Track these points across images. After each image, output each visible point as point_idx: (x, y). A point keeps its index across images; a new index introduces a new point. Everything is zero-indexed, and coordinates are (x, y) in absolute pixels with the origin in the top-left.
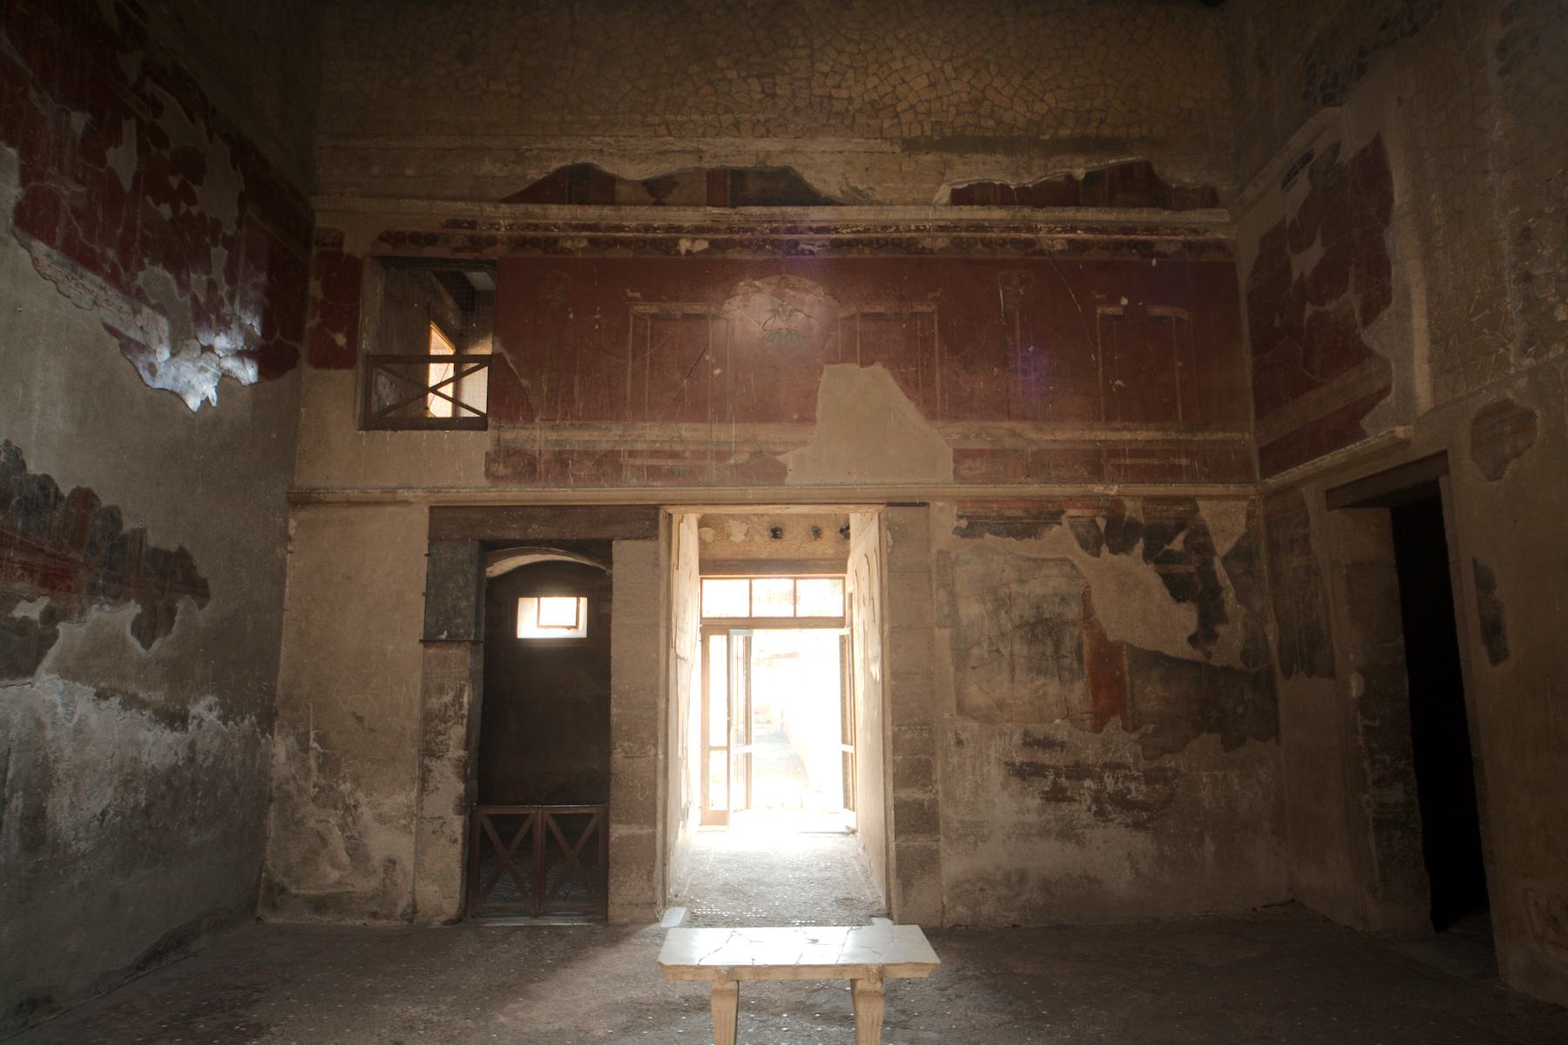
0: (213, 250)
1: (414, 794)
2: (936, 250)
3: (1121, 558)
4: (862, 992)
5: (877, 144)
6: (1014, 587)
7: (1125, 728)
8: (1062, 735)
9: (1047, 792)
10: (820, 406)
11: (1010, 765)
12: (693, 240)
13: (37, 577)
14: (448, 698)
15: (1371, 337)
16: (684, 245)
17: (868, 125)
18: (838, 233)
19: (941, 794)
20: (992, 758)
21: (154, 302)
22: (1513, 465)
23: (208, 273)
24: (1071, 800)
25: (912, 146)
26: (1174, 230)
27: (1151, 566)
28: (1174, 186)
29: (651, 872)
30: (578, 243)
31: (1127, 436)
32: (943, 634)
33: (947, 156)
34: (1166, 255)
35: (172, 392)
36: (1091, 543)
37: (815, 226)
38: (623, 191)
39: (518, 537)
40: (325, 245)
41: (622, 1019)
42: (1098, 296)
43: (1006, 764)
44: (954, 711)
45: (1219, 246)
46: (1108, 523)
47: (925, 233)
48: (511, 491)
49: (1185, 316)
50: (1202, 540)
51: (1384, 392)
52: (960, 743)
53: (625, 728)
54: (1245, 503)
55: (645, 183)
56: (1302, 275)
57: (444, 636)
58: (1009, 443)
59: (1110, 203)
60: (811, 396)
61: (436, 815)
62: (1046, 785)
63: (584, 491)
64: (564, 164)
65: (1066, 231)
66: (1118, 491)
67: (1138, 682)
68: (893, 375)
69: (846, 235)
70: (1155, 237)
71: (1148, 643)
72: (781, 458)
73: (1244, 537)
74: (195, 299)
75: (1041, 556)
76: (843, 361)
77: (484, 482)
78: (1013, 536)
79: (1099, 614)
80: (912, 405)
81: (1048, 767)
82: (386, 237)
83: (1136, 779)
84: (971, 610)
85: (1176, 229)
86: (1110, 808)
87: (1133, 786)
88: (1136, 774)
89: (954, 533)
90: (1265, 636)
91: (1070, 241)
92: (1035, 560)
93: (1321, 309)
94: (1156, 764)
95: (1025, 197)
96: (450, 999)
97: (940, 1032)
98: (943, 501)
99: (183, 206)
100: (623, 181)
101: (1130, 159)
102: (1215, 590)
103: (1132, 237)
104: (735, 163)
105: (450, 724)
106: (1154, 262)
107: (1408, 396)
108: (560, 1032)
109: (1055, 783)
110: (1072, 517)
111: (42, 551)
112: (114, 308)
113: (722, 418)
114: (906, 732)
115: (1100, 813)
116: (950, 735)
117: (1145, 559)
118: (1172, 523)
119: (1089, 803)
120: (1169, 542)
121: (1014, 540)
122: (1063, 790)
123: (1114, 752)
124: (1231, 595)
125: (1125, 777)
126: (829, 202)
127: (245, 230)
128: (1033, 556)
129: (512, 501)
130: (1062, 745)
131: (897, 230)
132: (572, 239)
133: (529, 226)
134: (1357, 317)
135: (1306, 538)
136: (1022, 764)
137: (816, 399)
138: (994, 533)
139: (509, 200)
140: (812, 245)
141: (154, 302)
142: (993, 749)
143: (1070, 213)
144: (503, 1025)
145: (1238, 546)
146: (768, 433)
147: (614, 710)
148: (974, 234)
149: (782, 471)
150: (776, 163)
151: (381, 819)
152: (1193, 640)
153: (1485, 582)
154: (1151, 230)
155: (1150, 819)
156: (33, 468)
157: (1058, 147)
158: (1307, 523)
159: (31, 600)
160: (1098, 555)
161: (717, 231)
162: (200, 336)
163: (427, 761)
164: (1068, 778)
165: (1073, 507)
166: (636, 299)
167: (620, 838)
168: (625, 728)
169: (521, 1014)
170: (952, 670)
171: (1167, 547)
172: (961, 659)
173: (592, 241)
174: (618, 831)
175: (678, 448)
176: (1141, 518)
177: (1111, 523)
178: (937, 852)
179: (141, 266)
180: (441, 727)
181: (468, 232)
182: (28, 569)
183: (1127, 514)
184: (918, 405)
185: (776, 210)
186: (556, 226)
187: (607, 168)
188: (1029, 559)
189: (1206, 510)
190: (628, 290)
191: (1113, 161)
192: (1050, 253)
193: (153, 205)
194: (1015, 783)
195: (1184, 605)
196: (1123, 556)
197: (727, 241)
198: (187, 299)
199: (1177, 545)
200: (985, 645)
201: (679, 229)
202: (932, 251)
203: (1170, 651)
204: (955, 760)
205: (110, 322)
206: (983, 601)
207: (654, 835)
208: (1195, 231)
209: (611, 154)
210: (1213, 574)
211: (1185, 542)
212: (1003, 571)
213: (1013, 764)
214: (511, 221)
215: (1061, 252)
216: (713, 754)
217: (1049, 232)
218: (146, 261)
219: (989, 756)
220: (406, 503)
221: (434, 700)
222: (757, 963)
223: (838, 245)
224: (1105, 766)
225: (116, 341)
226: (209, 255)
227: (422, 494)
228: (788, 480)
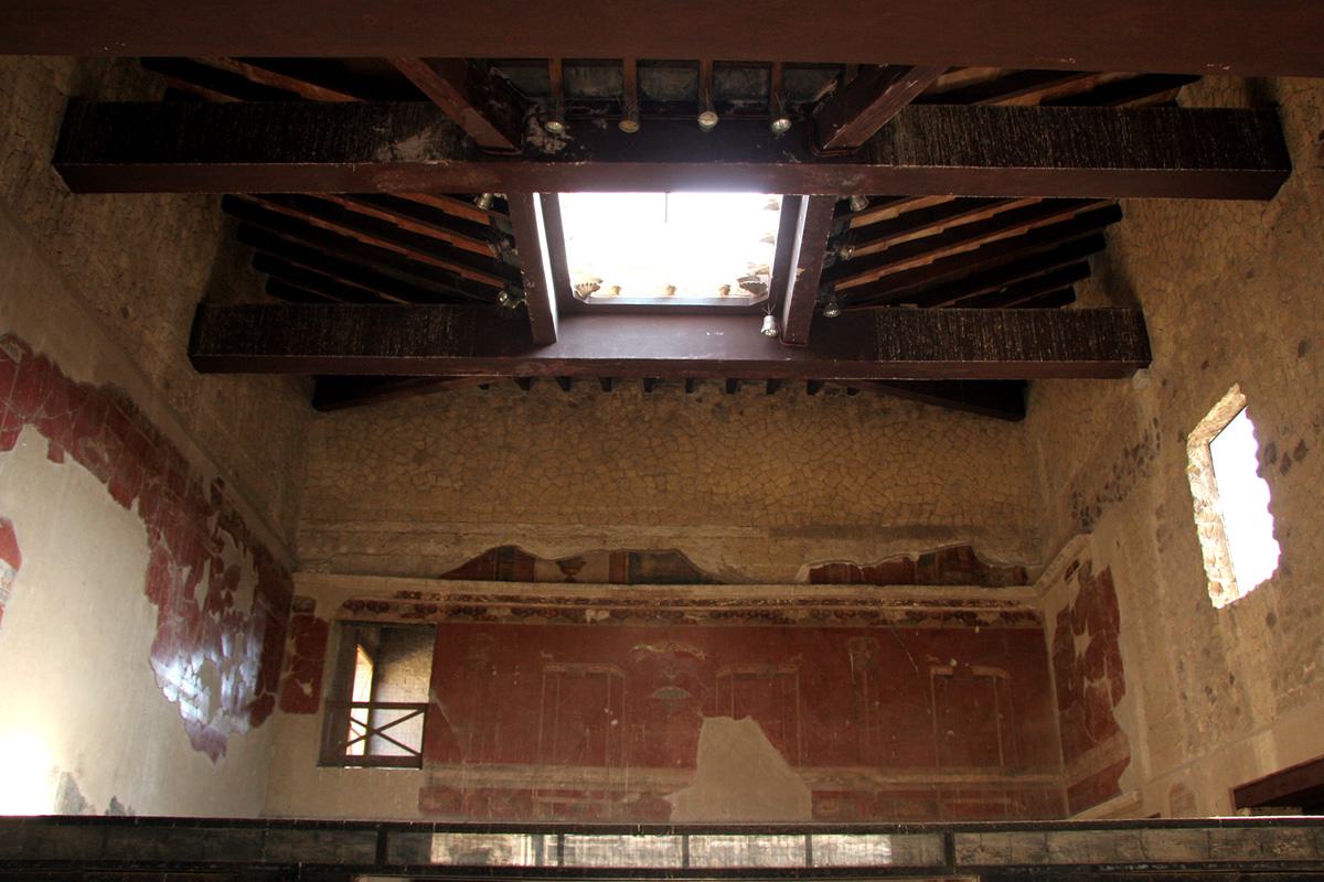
2: (797, 620)
12: (597, 611)
16: (590, 614)
17: (742, 516)
18: (716, 605)
26: (993, 603)
28: (991, 566)
30: (502, 612)
34: (986, 624)
37: (697, 599)
38: (540, 569)
40: (300, 610)
45: (1030, 616)
47: (788, 607)
55: (559, 562)
64: (493, 546)
69: (722, 608)
70: (977, 609)
82: (348, 605)
85: (994, 601)
91: (908, 613)
100: (541, 560)
101: (956, 543)
103: (959, 609)
106: (977, 629)
126: (708, 580)
132: (498, 608)
140: (695, 615)
148: (830, 607)
154: (973, 603)
157: (898, 533)
166: (548, 660)
173: (514, 610)
181: (414, 602)
185: (665, 587)
186: (485, 597)
190: (542, 652)
191: (942, 545)
192: (892, 623)
201: (586, 601)
202: (794, 622)
208: (1010, 603)
209: (532, 539)
214: (449, 593)
215: (900, 621)
217: (890, 605)
223: (717, 615)
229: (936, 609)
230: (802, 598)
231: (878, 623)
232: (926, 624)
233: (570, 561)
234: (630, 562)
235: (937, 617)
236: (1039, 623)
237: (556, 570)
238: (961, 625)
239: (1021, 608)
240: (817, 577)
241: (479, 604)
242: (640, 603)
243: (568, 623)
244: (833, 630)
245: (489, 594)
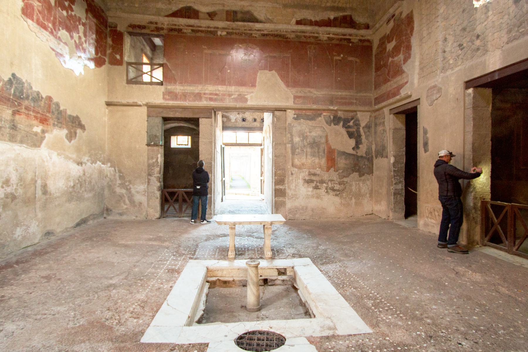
0: (79, 27)
3: (337, 127)
4: (267, 228)
5: (275, 5)
6: (308, 134)
7: (334, 171)
8: (318, 172)
10: (257, 82)
11: (305, 180)
12: (222, 32)
13: (39, 120)
15: (405, 68)
21: (64, 41)
22: (435, 102)
23: (78, 33)
24: (319, 189)
25: (285, 6)
26: (356, 36)
27: (344, 129)
30: (188, 31)
31: (340, 93)
32: (289, 146)
33: (295, 10)
34: (354, 43)
35: (71, 69)
36: (329, 123)
37: (257, 29)
42: (335, 54)
45: (368, 41)
47: (288, 33)
49: (358, 60)
50: (357, 122)
51: (406, 83)
54: (369, 113)
56: (389, 50)
58: (308, 94)
59: (340, 26)
60: (255, 79)
62: (313, 185)
65: (327, 34)
67: (339, 159)
68: (278, 74)
69: (266, 32)
71: (342, 150)
72: (246, 96)
73: (369, 122)
74: (75, 41)
75: (316, 125)
76: (264, 69)
79: (330, 142)
80: (283, 83)
84: (297, 139)
91: (328, 38)
92: (314, 127)
93: (393, 60)
95: (317, 24)
99: (70, 12)
100: (201, 12)
102: (360, 136)
103: (345, 37)
104: (234, 8)
106: (351, 45)
107: (412, 83)
109: (316, 185)
111: (39, 113)
112: (52, 42)
113: (230, 85)
116: (290, 172)
118: (350, 118)
120: (349, 122)
124: (364, 137)
126: (261, 22)
127: (88, 21)
130: (318, 175)
131: (280, 31)
132: (186, 29)
133: (173, 25)
134: (402, 62)
135: (384, 122)
137: (256, 80)
138: (303, 119)
139: (168, 16)
141: (64, 41)
143: (328, 29)
145: (367, 124)
146: (243, 89)
149: (246, 100)
150: (246, 9)
153: (425, 132)
154: (350, 35)
156: (34, 89)
158: (384, 118)
159: (37, 126)
160: (330, 126)
161: (229, 29)
162: (78, 53)
170: (291, 155)
171: (348, 124)
172: (293, 153)
173: (193, 30)
176: (343, 117)
177: (334, 117)
179: (59, 30)
182: (36, 118)
183: (339, 115)
184: (284, 83)
185: (246, 24)
186: (182, 25)
187: (196, 7)
188: (312, 126)
189: (359, 115)
193: (60, 10)
195: (351, 139)
196: (337, 126)
197: (231, 32)
198: (73, 41)
199: (351, 123)
201: (218, 28)
204: (291, 178)
205: (52, 47)
206: (299, 137)
208: (362, 36)
210: (359, 132)
211: (353, 123)
213: (306, 180)
215: (326, 40)
218: (60, 28)
223: (264, 35)
225: (54, 53)
226: (78, 28)
229: (338, 37)
230: (293, 30)
231: (318, 40)
232: (334, 42)
233: (212, 13)
234: (233, 14)
235: (338, 39)
236: (371, 44)
237: (207, 16)
238: (345, 43)
239: (366, 38)
240: (298, 23)
241: (179, 27)
242: (237, 29)
243: (212, 36)
244: (302, 42)
245: (183, 24)
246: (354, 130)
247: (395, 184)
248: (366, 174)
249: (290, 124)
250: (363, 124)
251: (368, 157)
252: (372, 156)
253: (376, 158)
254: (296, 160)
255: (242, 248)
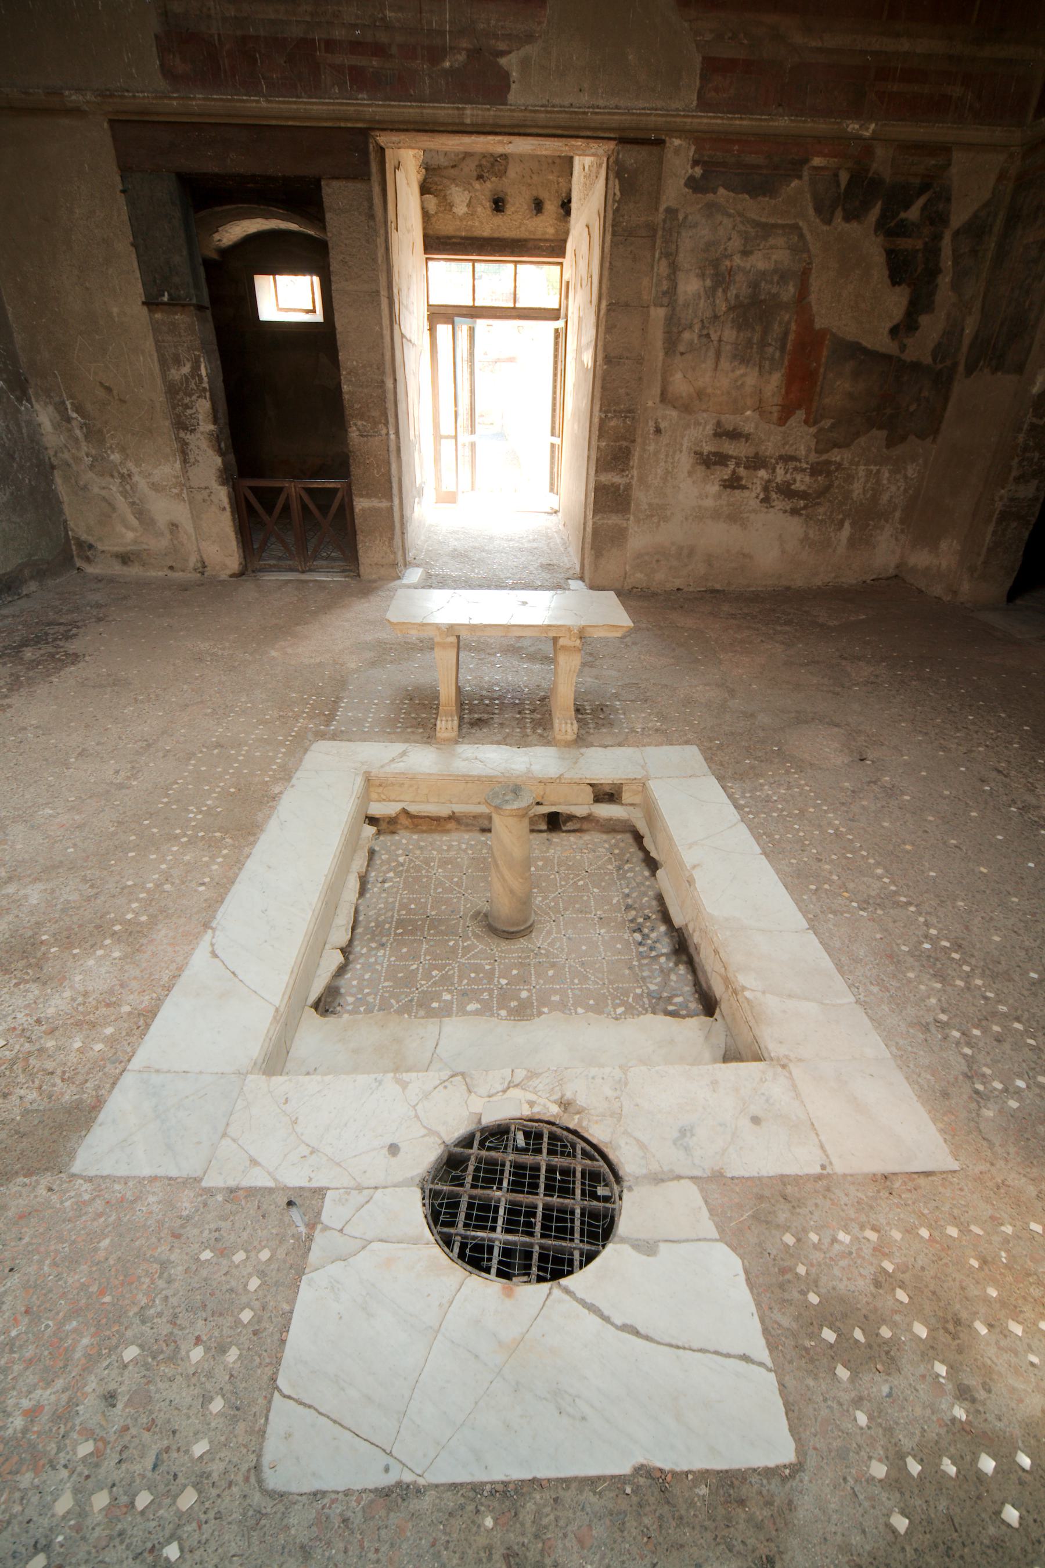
1: (178, 465)
3: (853, 229)
6: (737, 260)
7: (806, 422)
8: (749, 428)
9: (725, 480)
14: (186, 369)
19: (635, 479)
20: (684, 447)
24: (744, 488)
27: (880, 239)
29: (392, 539)
32: (658, 314)
39: (216, 170)
41: (369, 655)
43: (696, 453)
44: (658, 400)
46: (851, 177)
48: (194, 99)
52: (658, 431)
53: (357, 406)
57: (166, 299)
61: (203, 485)
62: (726, 473)
63: (279, 102)
66: (874, 131)
72: (503, 61)
77: (162, 85)
78: (748, 193)
79: (813, 297)
81: (731, 457)
83: (803, 470)
84: (690, 286)
86: (774, 496)
87: (799, 477)
88: (805, 466)
89: (686, 185)
90: (963, 330)
94: (824, 457)
96: (231, 637)
97: (619, 671)
98: (680, 137)
102: (933, 272)
105: (194, 397)
108: (320, 664)
109: (734, 472)
110: (815, 168)
114: (612, 418)
115: (766, 500)
116: (651, 423)
117: (876, 231)
119: (758, 491)
120: (907, 207)
121: (747, 197)
122: (739, 479)
123: (792, 445)
125: (795, 469)
128: (763, 220)
129: (200, 115)
130: (747, 437)
136: (710, 453)
142: (686, 438)
144: (274, 658)
147: (345, 388)
151: (155, 487)
152: (894, 331)
155: (805, 507)
160: (829, 222)
163: (182, 434)
164: (745, 468)
165: (820, 154)
167: (363, 510)
168: (357, 406)
169: (289, 650)
170: (661, 355)
171: (903, 215)
172: (671, 345)
174: (361, 504)
175: (383, 38)
177: (856, 178)
178: (626, 528)
180: (187, 400)
183: (875, 166)
194: (701, 470)
196: (855, 224)
199: (913, 214)
200: (697, 328)
203: (867, 343)
204: (652, 448)
206: (702, 276)
207: (391, 508)
211: (924, 208)
212: (730, 239)
213: (701, 454)
216: (443, 441)
219: (682, 445)
220: (76, 112)
221: (173, 371)
222: (474, 622)
224: (781, 457)
227: (93, 99)
228: (511, 97)
246: (919, 245)
247: (1017, 480)
248: (912, 437)
249: (671, 212)
250: (959, 216)
251: (940, 366)
252: (955, 365)
253: (970, 370)
254: (679, 376)
255: (482, 698)
